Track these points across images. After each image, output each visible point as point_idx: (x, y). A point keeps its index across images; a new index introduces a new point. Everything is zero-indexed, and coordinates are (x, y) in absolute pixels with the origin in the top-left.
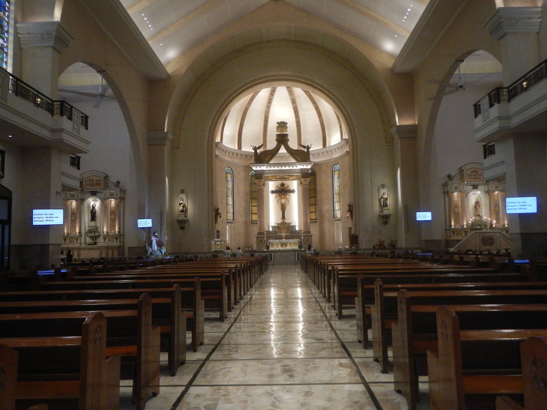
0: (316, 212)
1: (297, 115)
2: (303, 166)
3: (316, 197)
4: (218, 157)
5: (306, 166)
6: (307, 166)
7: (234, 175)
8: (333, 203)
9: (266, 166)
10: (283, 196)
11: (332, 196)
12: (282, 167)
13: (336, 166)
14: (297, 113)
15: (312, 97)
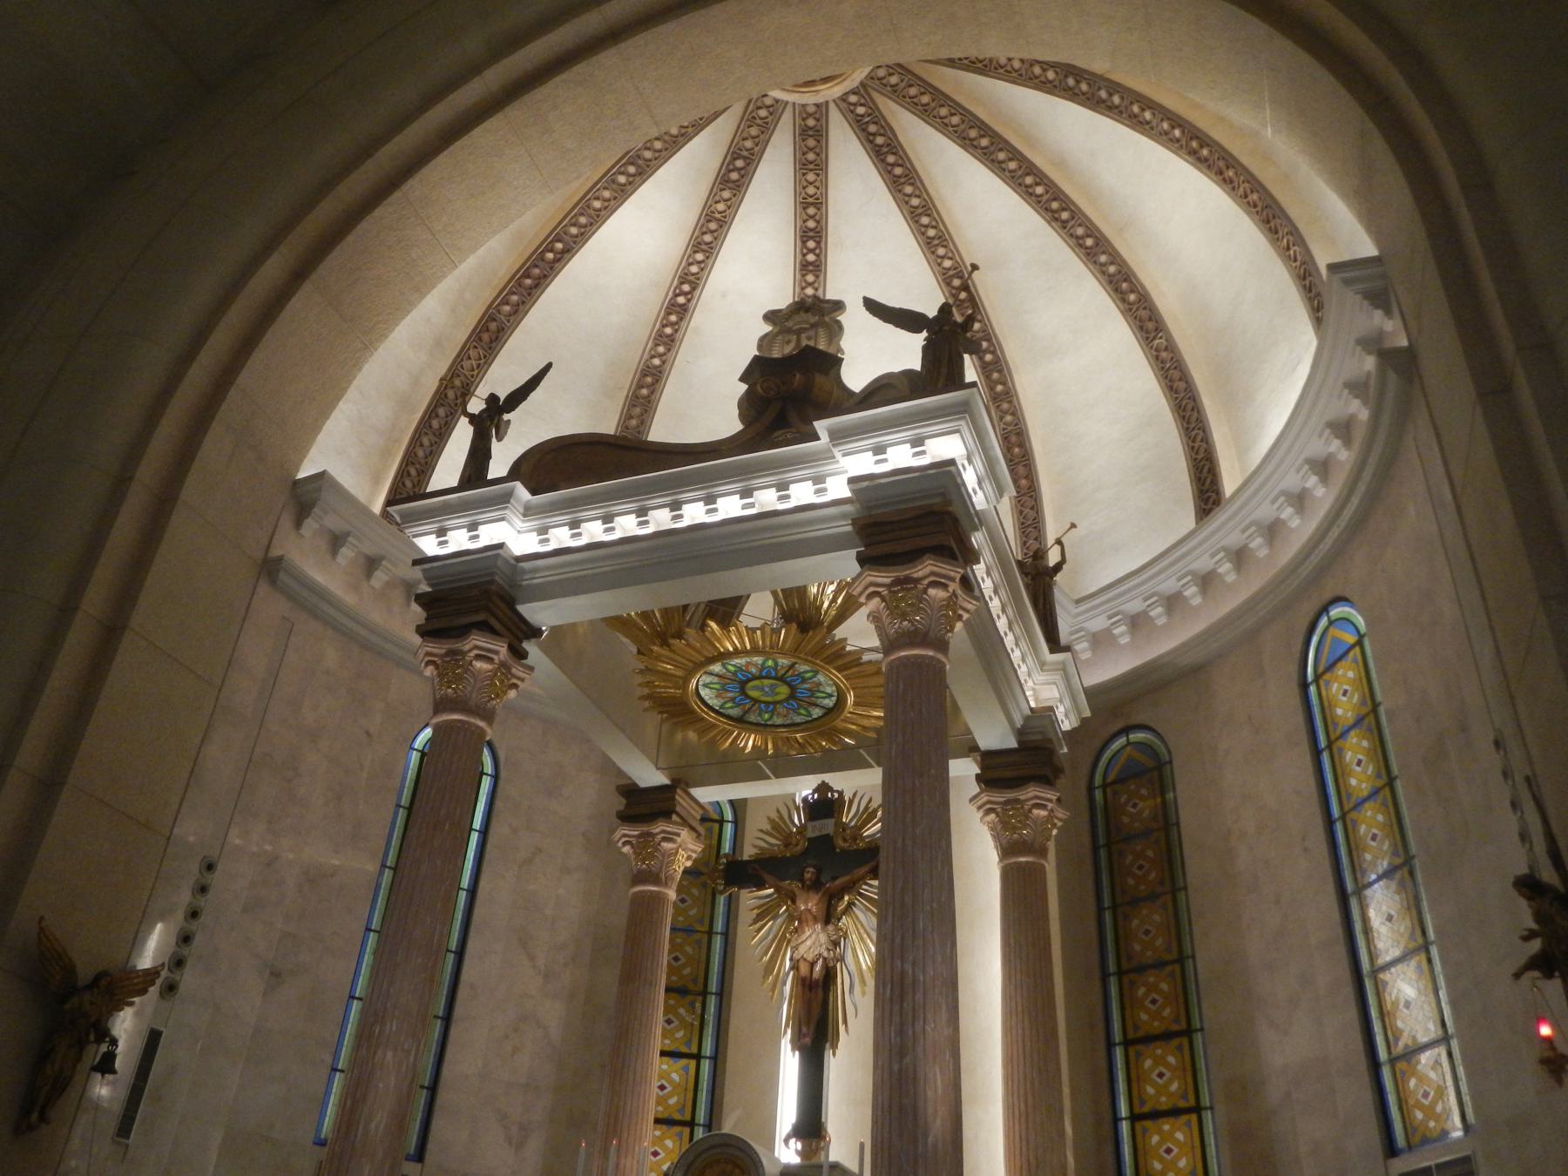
0: (1197, 1109)
1: (999, 388)
2: (879, 450)
3: (1179, 960)
4: (282, 575)
5: (906, 449)
6: (918, 442)
7: (501, 783)
8: (1348, 991)
9: (528, 512)
10: (810, 903)
11: (1336, 916)
12: (676, 506)
13: (1331, 623)
14: (1000, 371)
15: (1067, 203)
